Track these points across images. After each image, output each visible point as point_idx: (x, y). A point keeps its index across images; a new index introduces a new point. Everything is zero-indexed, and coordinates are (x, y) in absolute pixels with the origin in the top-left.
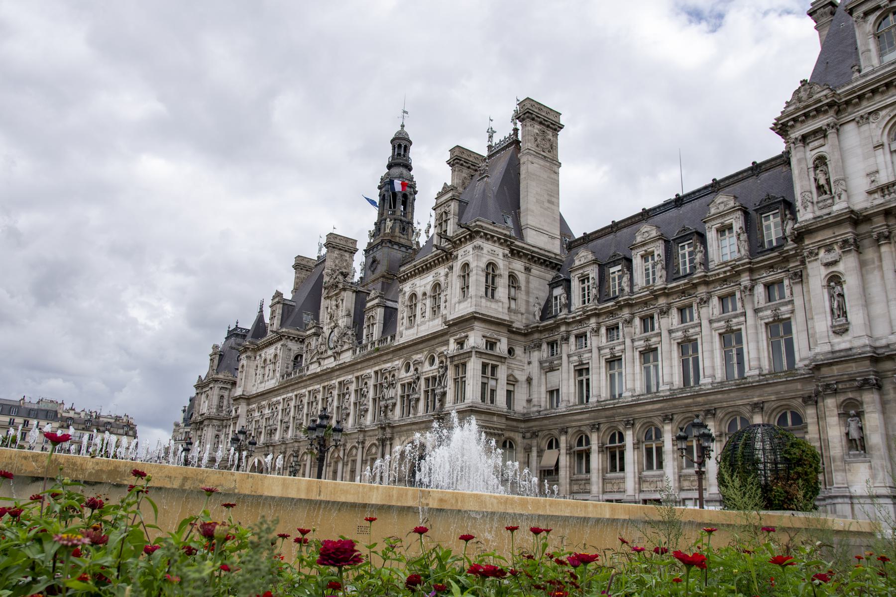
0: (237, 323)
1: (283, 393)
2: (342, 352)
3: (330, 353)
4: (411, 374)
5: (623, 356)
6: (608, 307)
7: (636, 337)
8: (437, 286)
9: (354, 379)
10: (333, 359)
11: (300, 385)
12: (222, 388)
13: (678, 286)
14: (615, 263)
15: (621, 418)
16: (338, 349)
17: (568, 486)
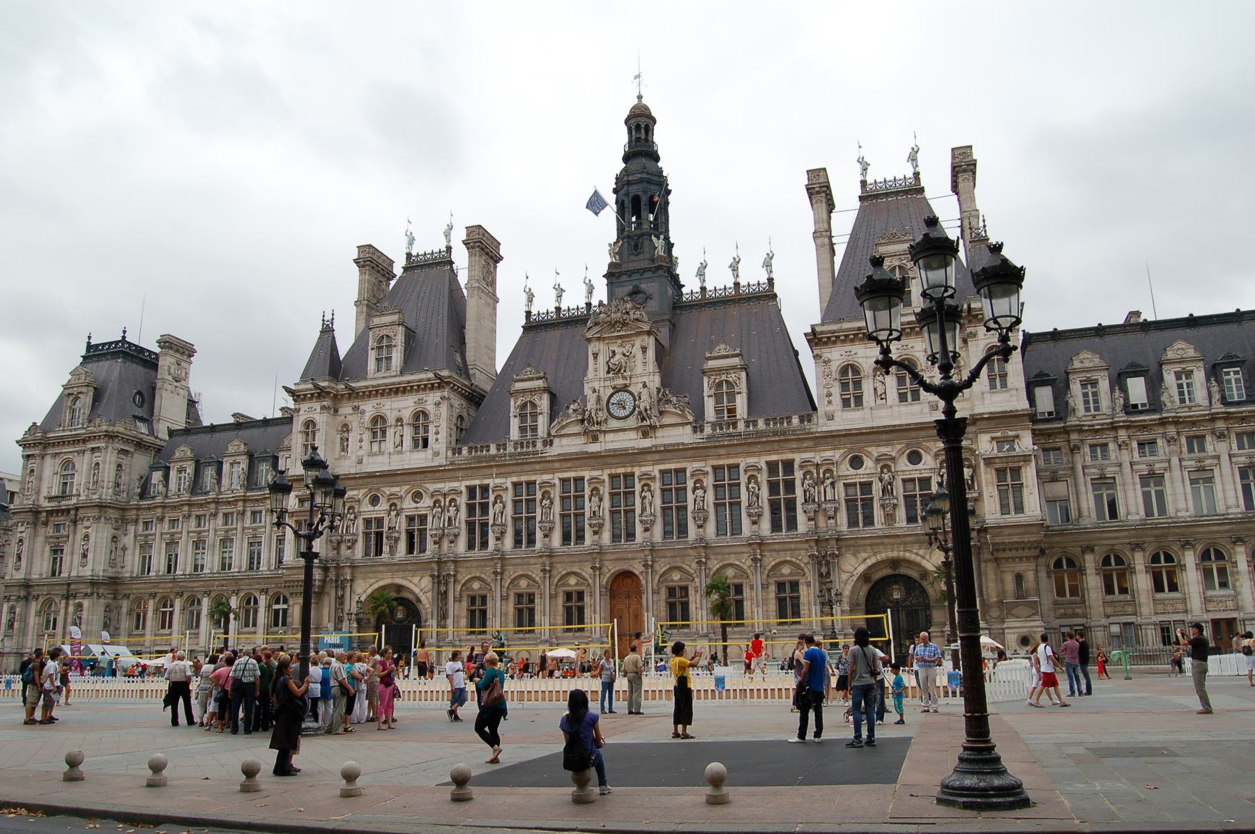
0: (124, 332)
1: (464, 478)
2: (662, 426)
3: (614, 424)
4: (869, 471)
5: (1167, 475)
6: (1145, 421)
7: (1184, 456)
9: (709, 469)
10: (633, 435)
11: (526, 468)
12: (123, 451)
13: (1241, 412)
14: (1135, 374)
15: (1175, 538)
16: (654, 421)
17: (1102, 609)
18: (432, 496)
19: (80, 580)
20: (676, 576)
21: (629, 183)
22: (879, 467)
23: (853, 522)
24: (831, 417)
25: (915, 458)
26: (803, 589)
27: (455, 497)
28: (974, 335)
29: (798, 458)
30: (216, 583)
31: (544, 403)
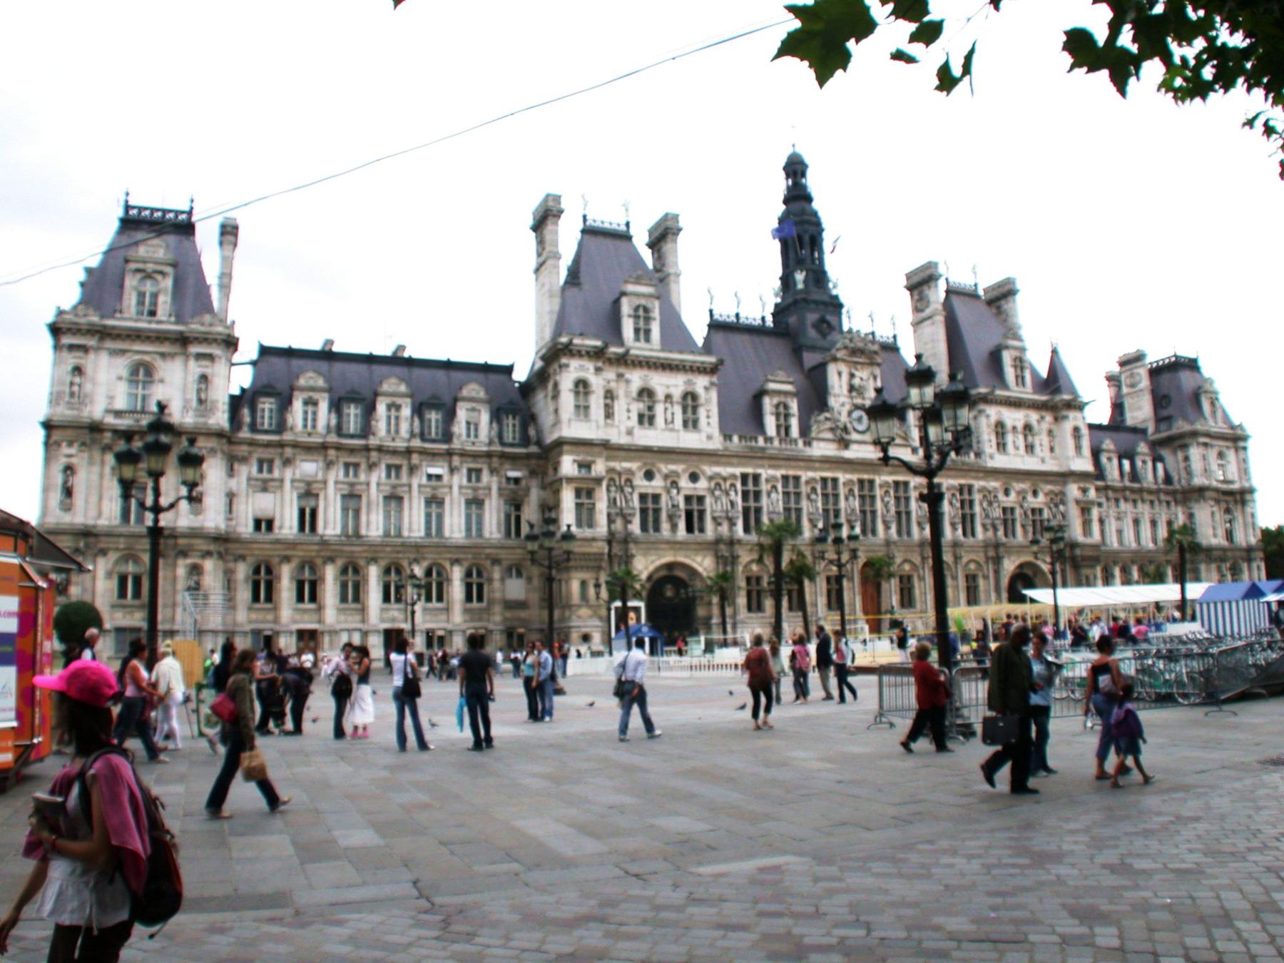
1: (739, 465)
8: (1028, 428)
10: (871, 448)
18: (710, 478)
19: (195, 533)
20: (907, 567)
21: (809, 223)
22: (1021, 498)
23: (1006, 535)
24: (991, 457)
25: (1035, 493)
26: (981, 582)
27: (734, 482)
28: (1065, 418)
29: (978, 484)
30: (388, 549)
31: (794, 406)
